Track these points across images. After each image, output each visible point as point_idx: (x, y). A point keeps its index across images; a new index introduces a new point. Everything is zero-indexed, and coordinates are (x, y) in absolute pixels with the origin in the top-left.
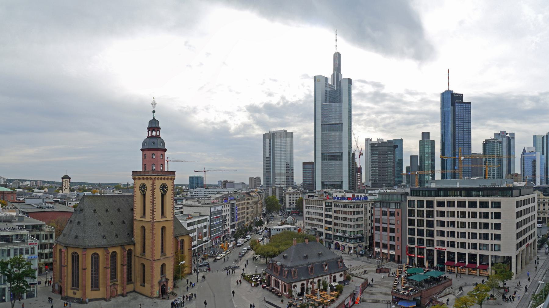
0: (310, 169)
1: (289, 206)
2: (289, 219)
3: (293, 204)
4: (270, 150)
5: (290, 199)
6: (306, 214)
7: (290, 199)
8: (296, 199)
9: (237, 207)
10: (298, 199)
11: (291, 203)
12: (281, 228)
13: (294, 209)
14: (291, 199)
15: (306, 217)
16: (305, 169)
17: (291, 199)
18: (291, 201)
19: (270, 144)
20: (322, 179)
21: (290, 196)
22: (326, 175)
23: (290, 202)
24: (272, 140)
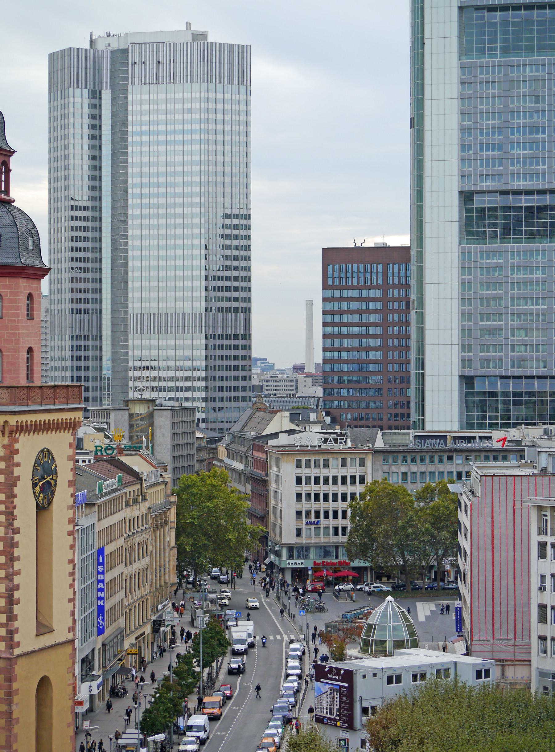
0: (374, 293)
1: (299, 533)
2: (384, 615)
3: (323, 522)
4: (96, 158)
5: (304, 489)
6: (542, 589)
7: (304, 489)
8: (349, 488)
9: (101, 551)
10: (359, 489)
11: (308, 513)
12: (407, 669)
13: (325, 551)
14: (313, 489)
15: (542, 607)
16: (337, 294)
17: (313, 489)
18: (313, 506)
19: (96, 117)
20: (464, 362)
21: (304, 472)
22: (491, 332)
23: (304, 506)
24: (106, 95)
